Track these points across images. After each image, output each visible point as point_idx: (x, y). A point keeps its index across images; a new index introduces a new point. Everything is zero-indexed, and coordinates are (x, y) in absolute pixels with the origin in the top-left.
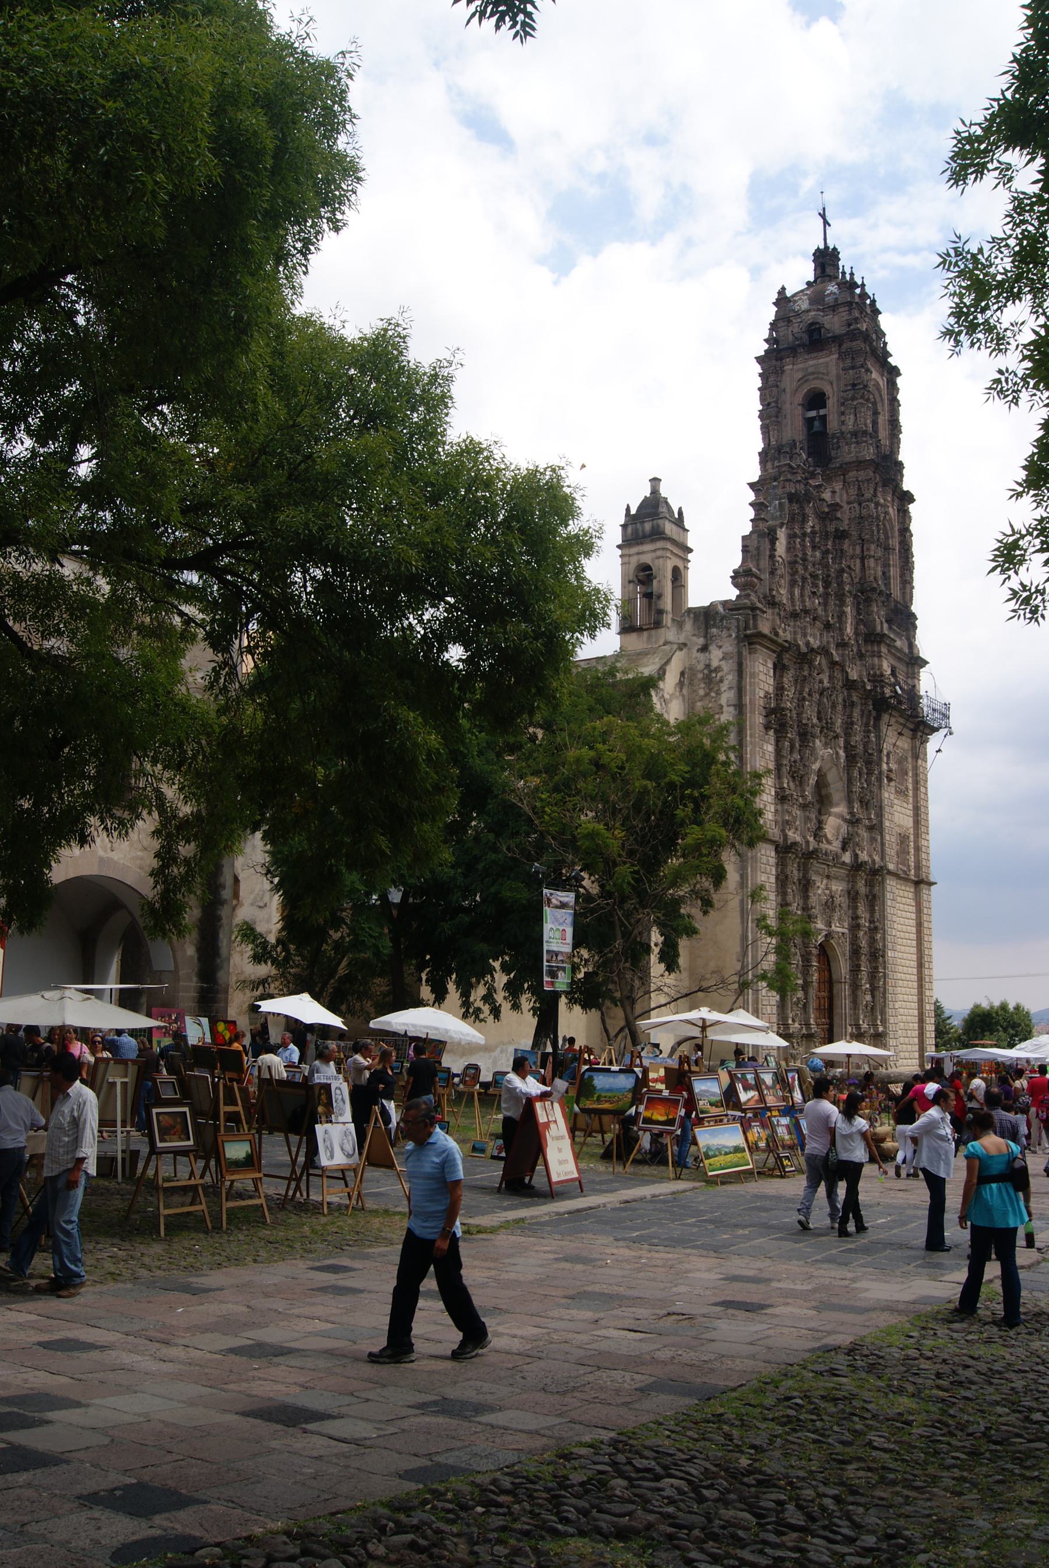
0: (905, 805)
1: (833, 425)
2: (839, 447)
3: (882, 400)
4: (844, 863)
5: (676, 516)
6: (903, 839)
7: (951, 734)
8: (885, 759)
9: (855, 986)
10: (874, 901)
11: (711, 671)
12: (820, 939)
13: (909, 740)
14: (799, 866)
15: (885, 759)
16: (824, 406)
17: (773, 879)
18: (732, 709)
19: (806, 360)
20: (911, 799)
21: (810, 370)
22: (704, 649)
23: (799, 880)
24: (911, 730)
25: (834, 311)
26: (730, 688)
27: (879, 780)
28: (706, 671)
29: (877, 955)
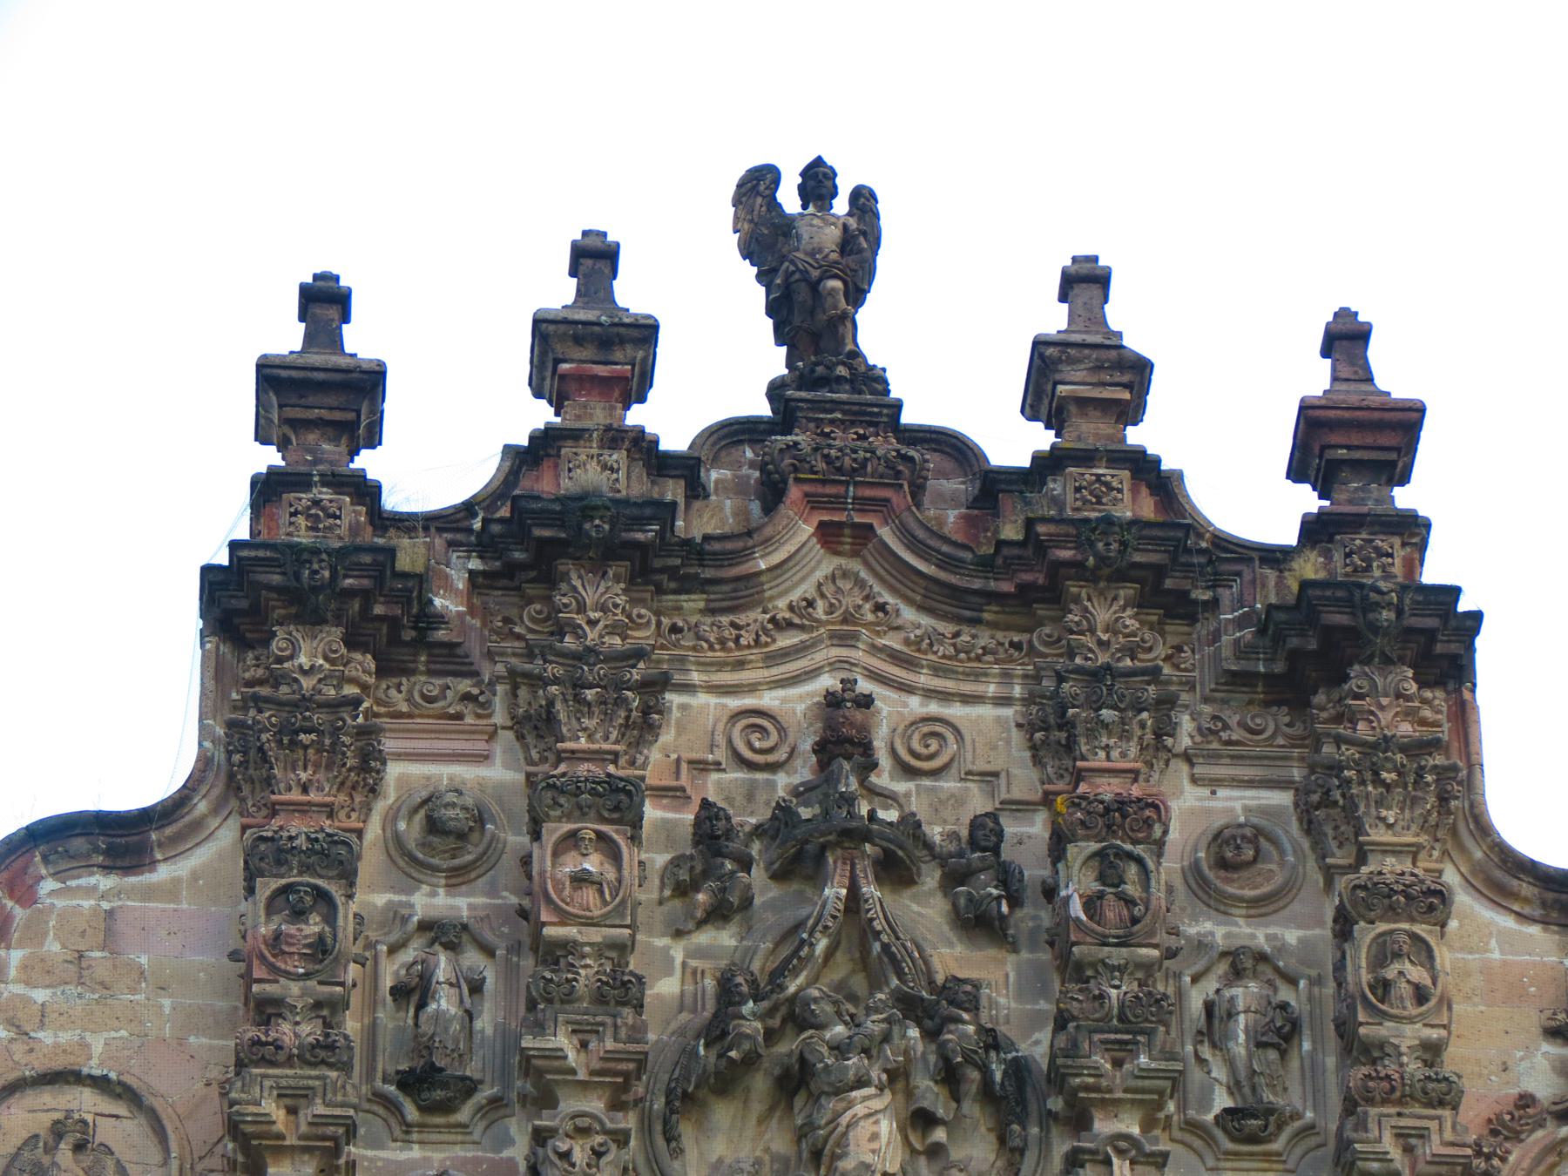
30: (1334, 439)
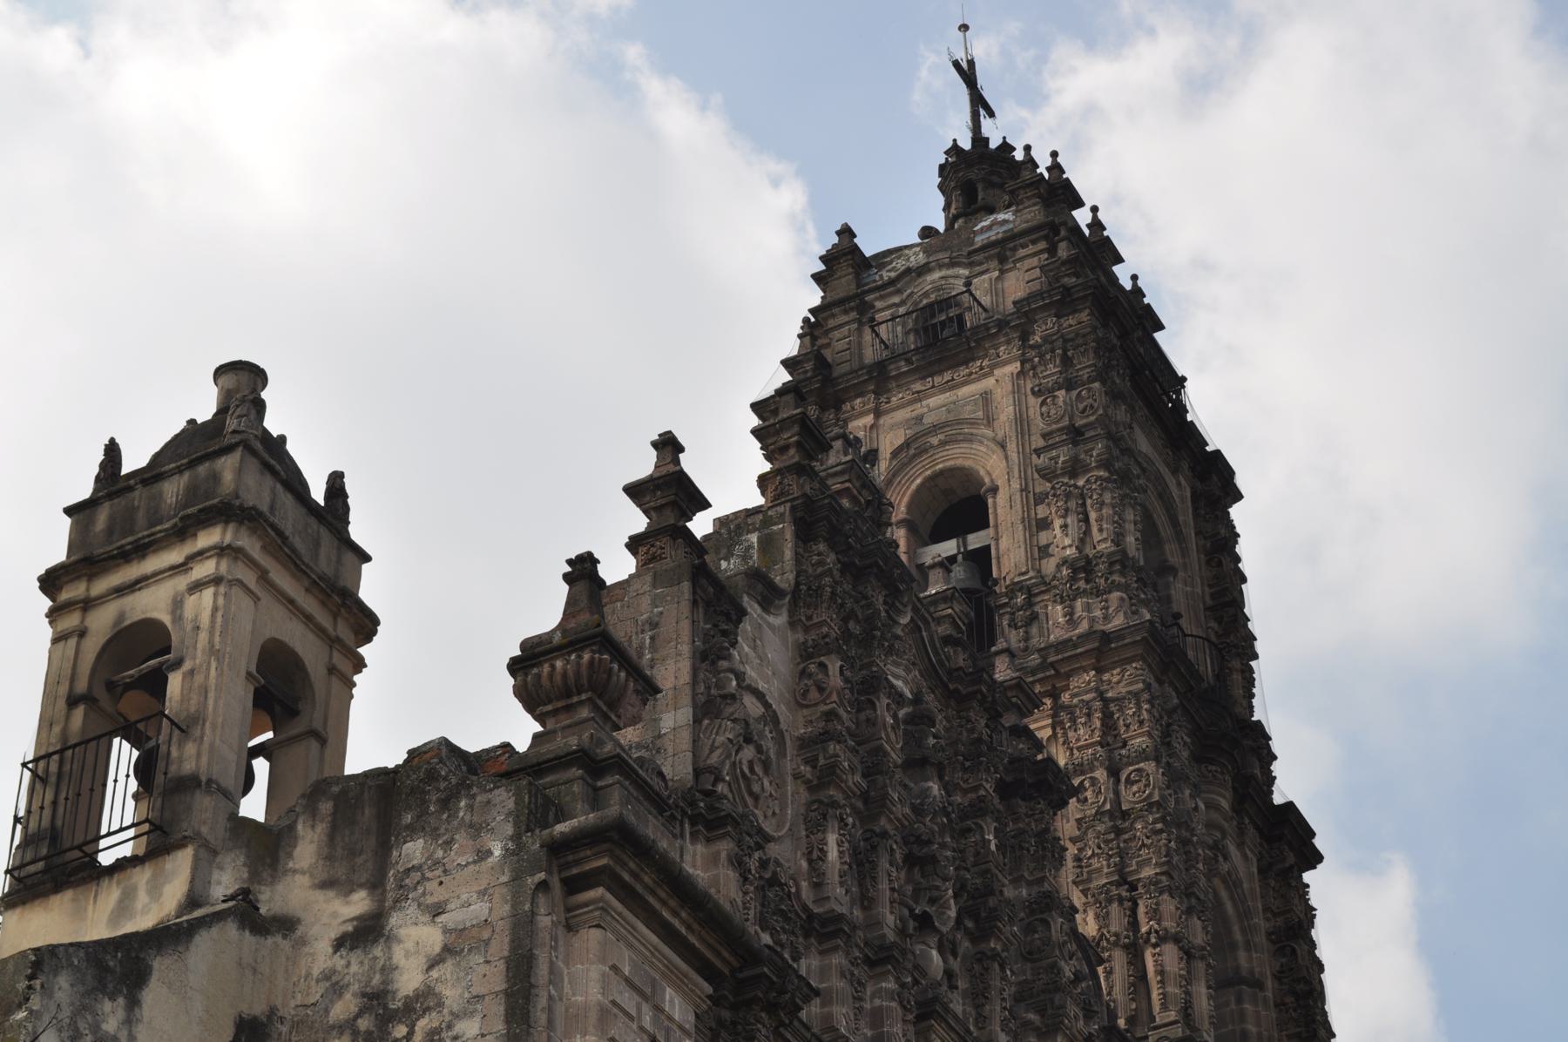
2: (1034, 617)
3: (1179, 537)
5: (318, 493)
11: (387, 1018)
16: (984, 525)
19: (919, 397)
21: (928, 420)
25: (1002, 260)
28: (364, 1024)
30: (1021, 696)
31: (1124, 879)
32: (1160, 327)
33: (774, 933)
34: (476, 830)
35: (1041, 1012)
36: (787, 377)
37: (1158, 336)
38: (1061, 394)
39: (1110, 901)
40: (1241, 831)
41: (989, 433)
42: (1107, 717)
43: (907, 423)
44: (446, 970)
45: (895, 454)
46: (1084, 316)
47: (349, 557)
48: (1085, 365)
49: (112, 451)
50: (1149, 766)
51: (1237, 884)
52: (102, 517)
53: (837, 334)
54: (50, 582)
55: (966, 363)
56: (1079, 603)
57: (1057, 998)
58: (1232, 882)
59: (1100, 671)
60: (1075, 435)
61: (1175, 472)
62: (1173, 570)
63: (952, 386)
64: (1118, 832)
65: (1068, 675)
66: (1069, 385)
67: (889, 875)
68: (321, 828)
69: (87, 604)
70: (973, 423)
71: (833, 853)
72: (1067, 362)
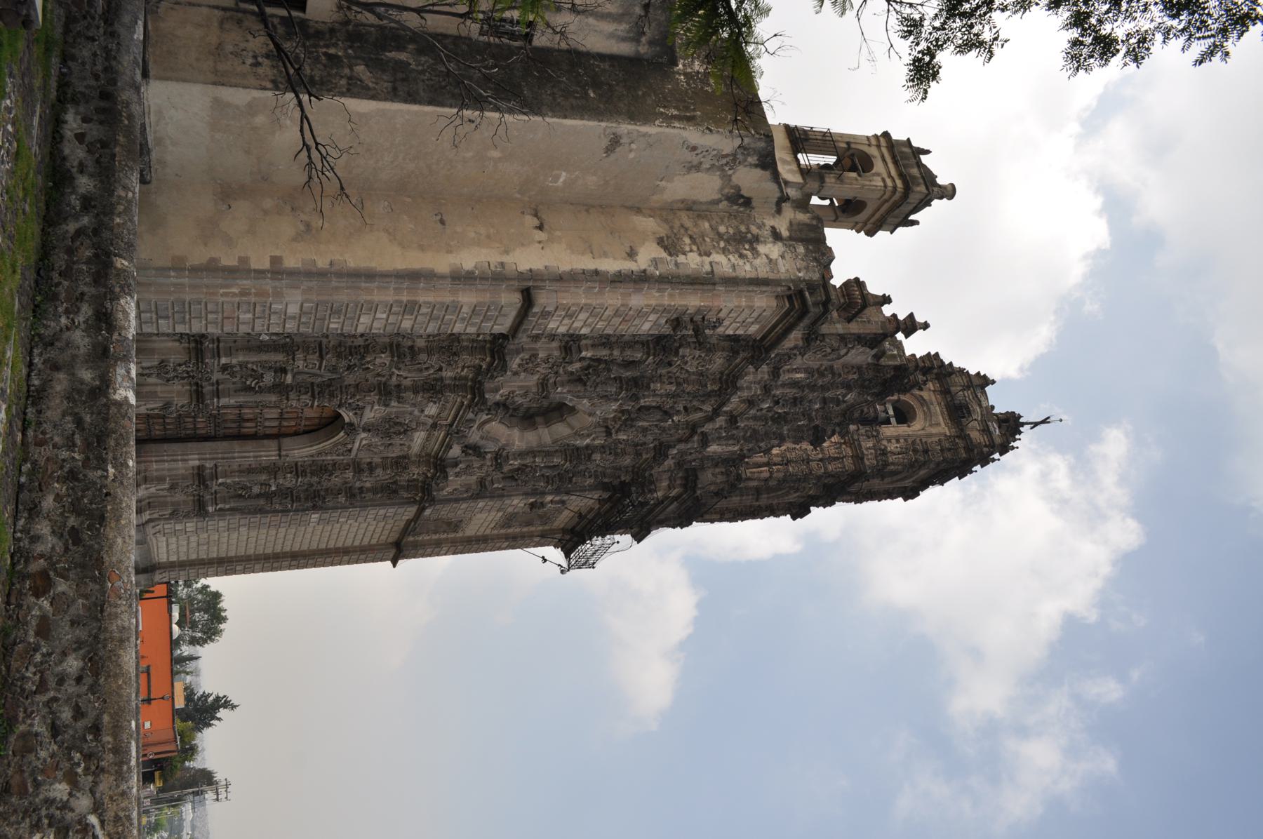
0: (492, 526)
1: (887, 431)
2: (869, 437)
3: (892, 482)
4: (449, 447)
5: (912, 217)
6: (455, 526)
7: (562, 572)
8: (557, 498)
9: (273, 470)
10: (389, 492)
11: (751, 243)
12: (347, 416)
13: (561, 526)
14: (461, 378)
15: (557, 498)
16: (898, 422)
17: (458, 328)
18: (707, 268)
19: (939, 404)
20: (495, 532)
22: (776, 236)
23: (442, 379)
24: (574, 527)
25: (983, 431)
26: (734, 266)
27: (534, 492)
28: (749, 236)
29: (314, 500)
31: (788, 462)
32: (960, 479)
33: (775, 357)
34: (807, 268)
35: (750, 436)
36: (947, 363)
37: (957, 478)
38: (939, 448)
39: (783, 458)
40: (803, 497)
41: (928, 424)
42: (837, 459)
43: (931, 400)
44: (765, 260)
45: (921, 396)
46: (964, 455)
47: (892, 227)
48: (949, 455)
49: (928, 152)
50: (823, 471)
51: (787, 495)
52: (907, 150)
53: (960, 379)
54: (886, 135)
55: (950, 418)
56: (873, 451)
57: (754, 441)
58: (787, 494)
59: (852, 457)
60: (926, 451)
61: (913, 481)
62: (883, 480)
63: (942, 414)
64: (803, 461)
65: (851, 447)
66: (942, 450)
67: (791, 392)
68: (808, 221)
69: (879, 146)
70: (930, 420)
71: (798, 376)
72: (949, 450)
